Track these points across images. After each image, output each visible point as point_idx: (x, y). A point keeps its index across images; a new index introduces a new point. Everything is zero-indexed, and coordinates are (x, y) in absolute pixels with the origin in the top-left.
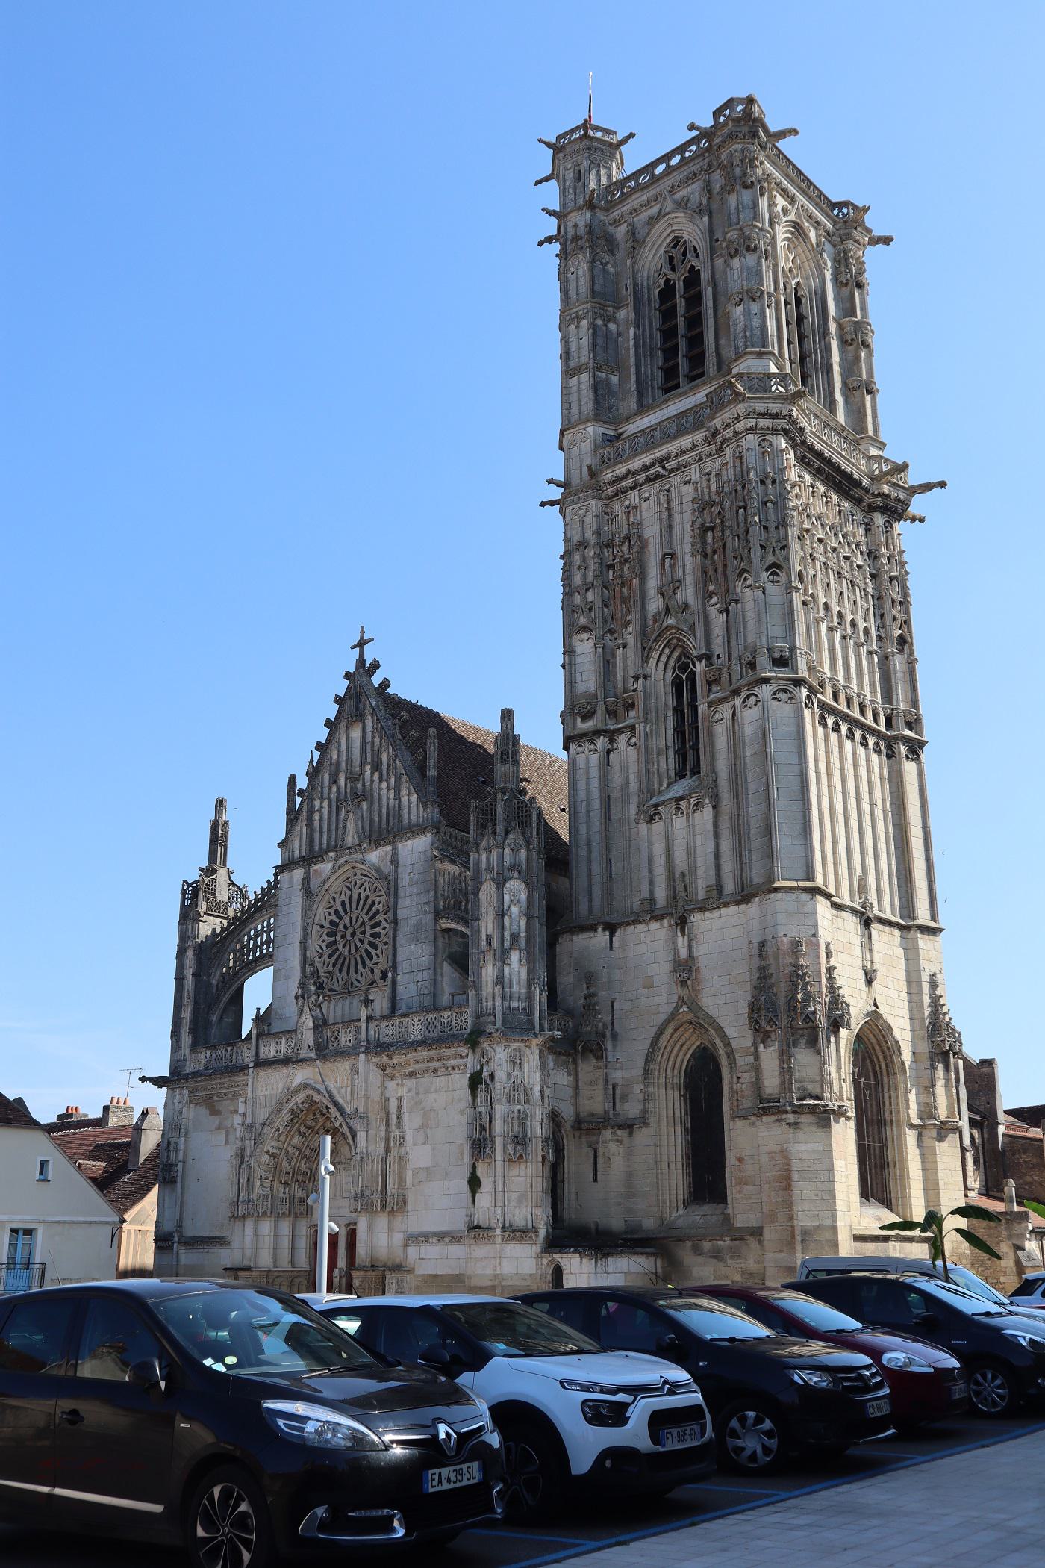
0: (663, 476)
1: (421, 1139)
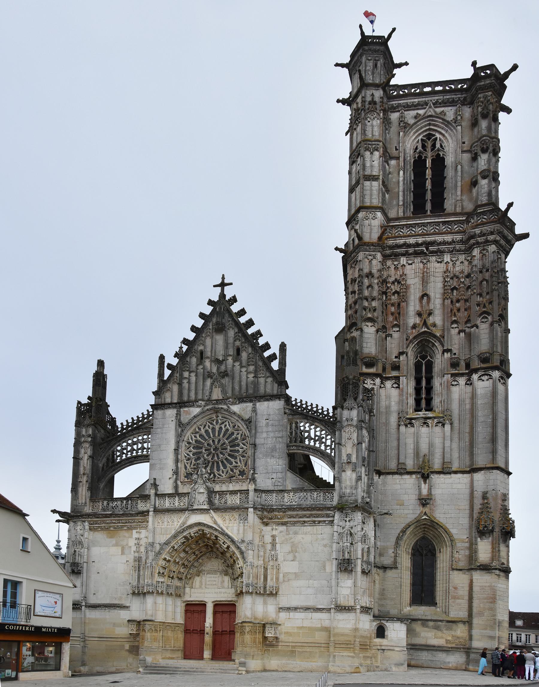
0: (425, 253)
1: (291, 557)
